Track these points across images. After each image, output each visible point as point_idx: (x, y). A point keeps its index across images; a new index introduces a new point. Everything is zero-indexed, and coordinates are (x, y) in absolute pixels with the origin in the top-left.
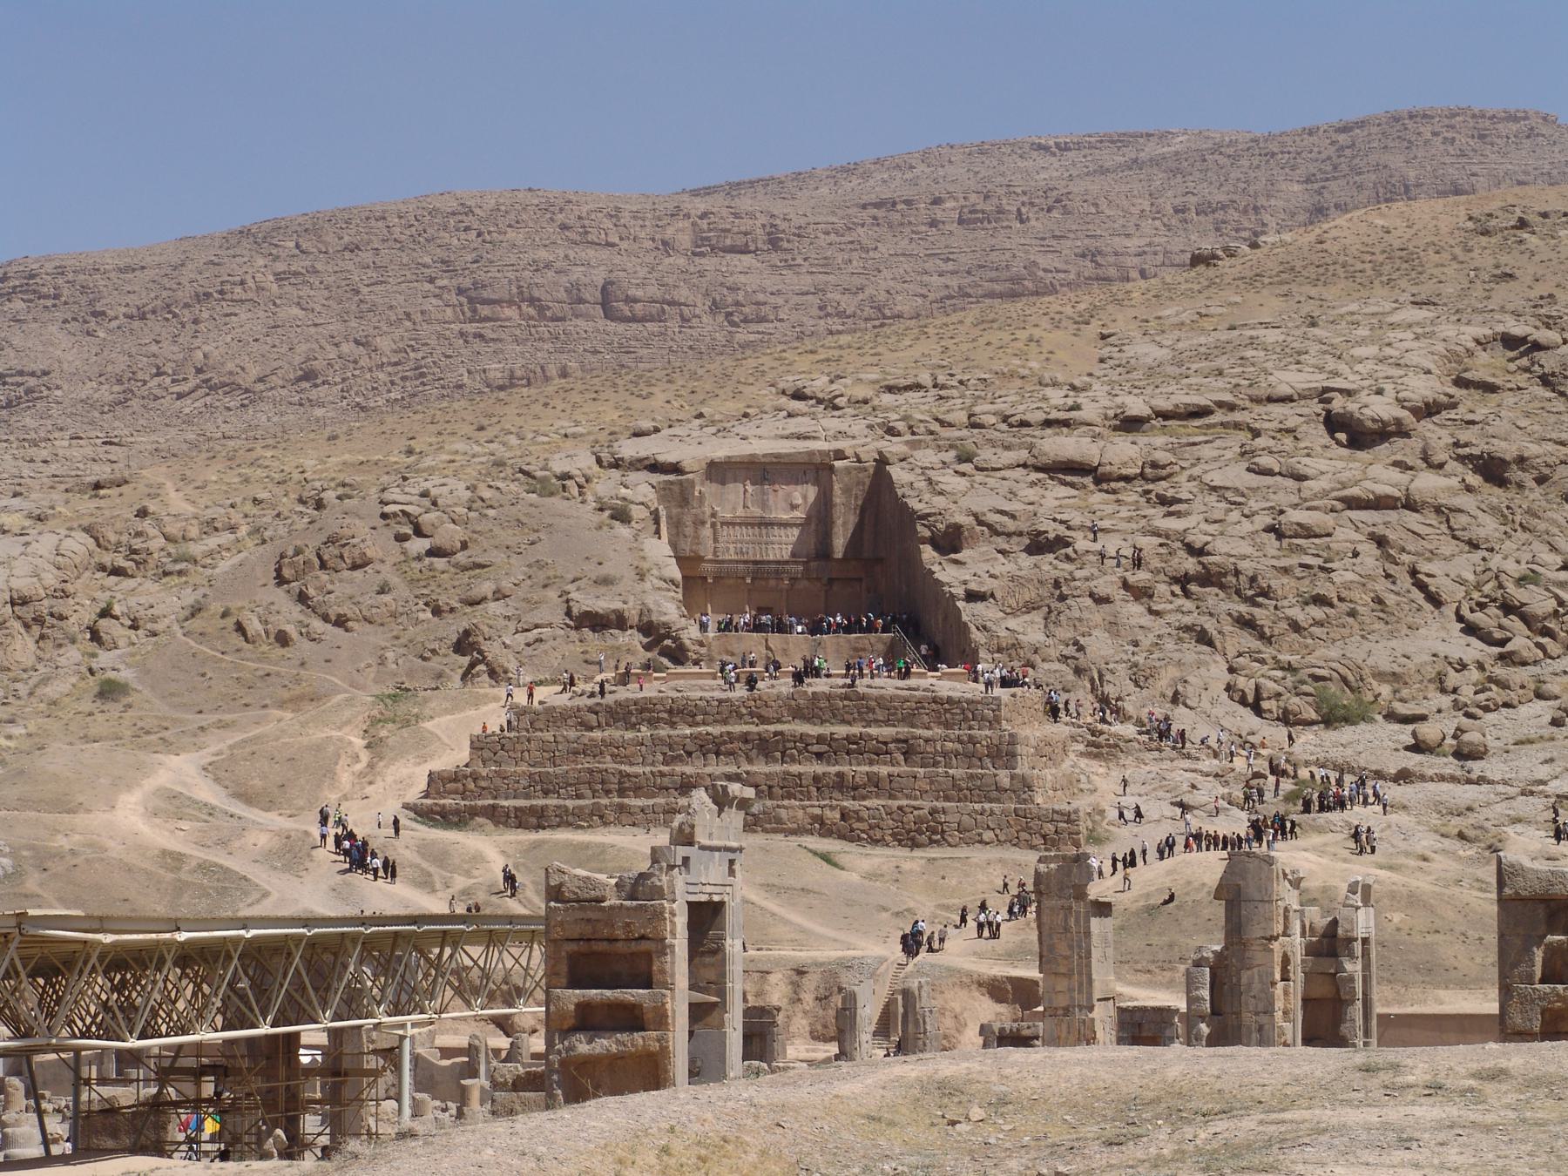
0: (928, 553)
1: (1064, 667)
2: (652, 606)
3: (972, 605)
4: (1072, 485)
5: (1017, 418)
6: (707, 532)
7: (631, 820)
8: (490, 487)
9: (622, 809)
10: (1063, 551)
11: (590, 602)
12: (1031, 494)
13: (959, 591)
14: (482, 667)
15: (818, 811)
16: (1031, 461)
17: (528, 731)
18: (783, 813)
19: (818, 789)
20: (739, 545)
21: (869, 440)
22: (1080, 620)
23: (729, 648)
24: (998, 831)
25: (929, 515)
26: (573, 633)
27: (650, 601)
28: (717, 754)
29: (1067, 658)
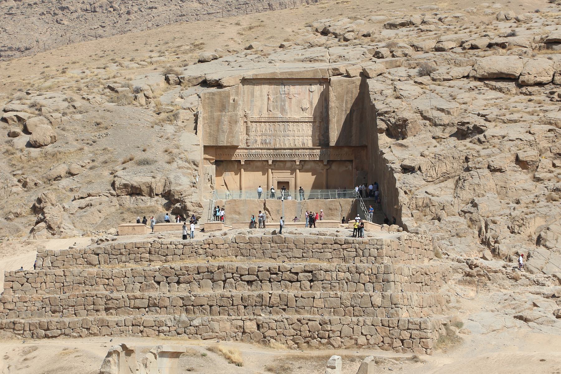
0: (383, 140)
1: (462, 220)
2: (172, 180)
3: (405, 175)
4: (500, 90)
5: (469, 43)
6: (241, 127)
7: (109, 331)
8: (84, 98)
9: (104, 324)
10: (478, 136)
11: (128, 178)
12: (465, 96)
13: (397, 166)
14: (42, 224)
15: (240, 323)
16: (473, 73)
17: (49, 268)
18: (216, 325)
19: (245, 307)
20: (264, 137)
21: (359, 61)
22: (478, 185)
23: (237, 210)
24: (368, 337)
25: (386, 112)
26: (115, 199)
27: (172, 177)
28: (178, 283)
29: (465, 213)
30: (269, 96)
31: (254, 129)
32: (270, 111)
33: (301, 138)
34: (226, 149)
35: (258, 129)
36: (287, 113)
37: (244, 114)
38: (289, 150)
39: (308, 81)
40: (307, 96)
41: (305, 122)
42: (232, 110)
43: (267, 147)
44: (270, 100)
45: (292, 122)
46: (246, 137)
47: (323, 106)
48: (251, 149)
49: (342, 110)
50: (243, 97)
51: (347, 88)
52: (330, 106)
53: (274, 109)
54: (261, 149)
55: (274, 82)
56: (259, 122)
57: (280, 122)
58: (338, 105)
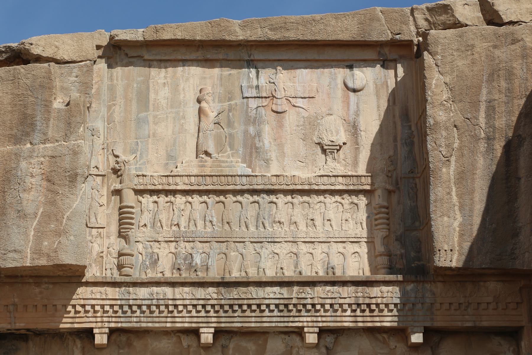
20: (184, 248)
30: (204, 104)
31: (146, 218)
32: (207, 153)
33: (319, 249)
34: (38, 284)
35: (163, 217)
36: (267, 161)
37: (112, 164)
38: (276, 289)
39: (338, 54)
40: (338, 106)
41: (333, 192)
42: (57, 136)
43: (193, 277)
44: (206, 115)
45: (286, 192)
46: (117, 244)
47: (395, 140)
48: (135, 284)
49: (476, 138)
50: (109, 108)
51: (491, 58)
52: (431, 121)
53: (220, 149)
54: (173, 284)
55: (221, 57)
56: (167, 192)
57: (242, 192)
58: (459, 119)
